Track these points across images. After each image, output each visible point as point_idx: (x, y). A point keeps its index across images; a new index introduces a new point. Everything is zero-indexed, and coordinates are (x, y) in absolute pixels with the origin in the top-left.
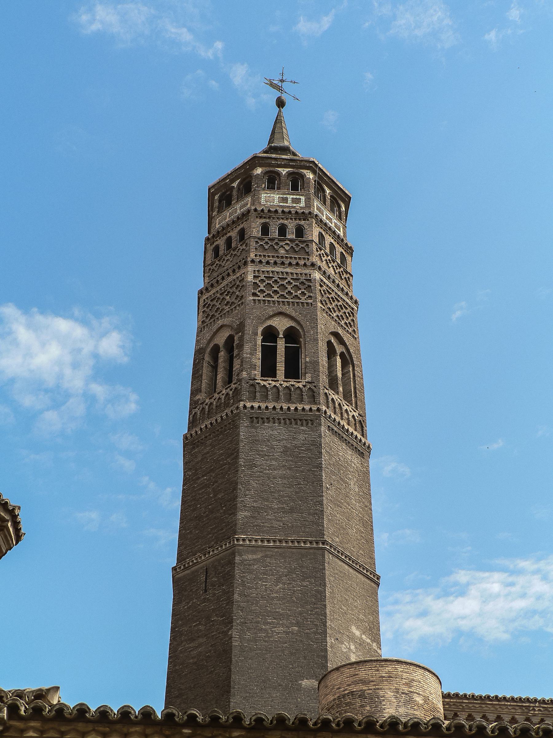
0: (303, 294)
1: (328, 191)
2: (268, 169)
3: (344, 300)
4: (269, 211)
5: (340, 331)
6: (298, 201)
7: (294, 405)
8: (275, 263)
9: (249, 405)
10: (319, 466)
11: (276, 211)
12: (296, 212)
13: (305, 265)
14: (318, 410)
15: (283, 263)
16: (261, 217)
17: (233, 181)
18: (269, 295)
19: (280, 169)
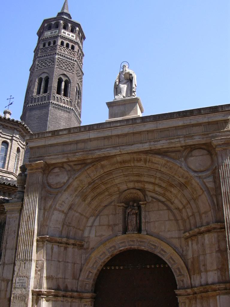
0: (52, 64)
1: (70, 25)
2: (48, 23)
3: (70, 62)
4: (46, 38)
5: (65, 73)
6: (56, 31)
7: (42, 102)
8: (44, 56)
9: (29, 105)
10: (47, 120)
11: (48, 38)
12: (54, 36)
13: (53, 54)
14: (49, 102)
15: (47, 55)
16: (43, 41)
17: (41, 30)
18: (41, 67)
19: (52, 22)
